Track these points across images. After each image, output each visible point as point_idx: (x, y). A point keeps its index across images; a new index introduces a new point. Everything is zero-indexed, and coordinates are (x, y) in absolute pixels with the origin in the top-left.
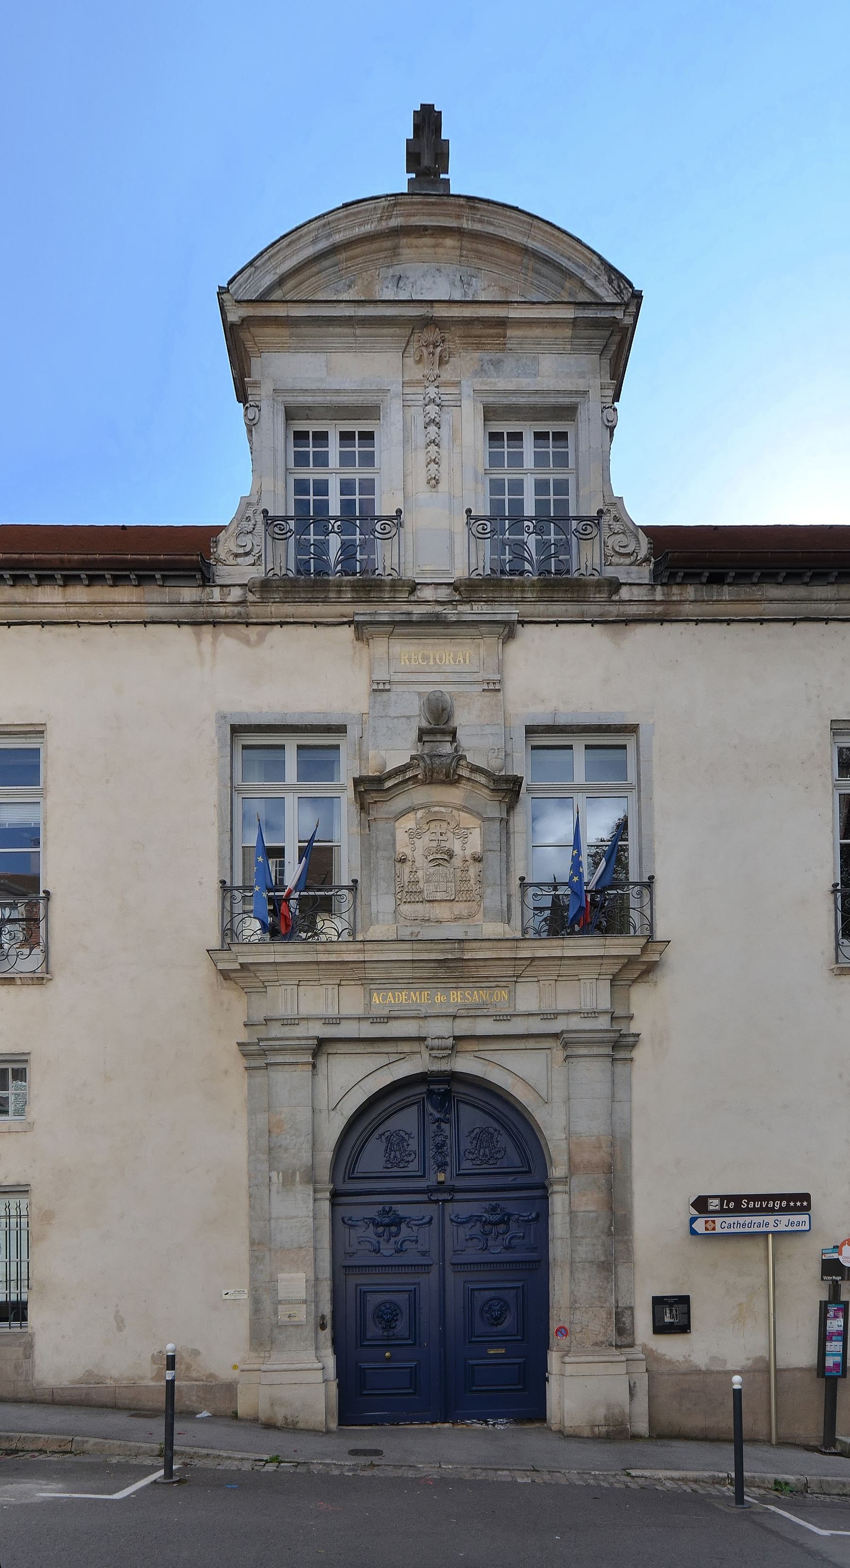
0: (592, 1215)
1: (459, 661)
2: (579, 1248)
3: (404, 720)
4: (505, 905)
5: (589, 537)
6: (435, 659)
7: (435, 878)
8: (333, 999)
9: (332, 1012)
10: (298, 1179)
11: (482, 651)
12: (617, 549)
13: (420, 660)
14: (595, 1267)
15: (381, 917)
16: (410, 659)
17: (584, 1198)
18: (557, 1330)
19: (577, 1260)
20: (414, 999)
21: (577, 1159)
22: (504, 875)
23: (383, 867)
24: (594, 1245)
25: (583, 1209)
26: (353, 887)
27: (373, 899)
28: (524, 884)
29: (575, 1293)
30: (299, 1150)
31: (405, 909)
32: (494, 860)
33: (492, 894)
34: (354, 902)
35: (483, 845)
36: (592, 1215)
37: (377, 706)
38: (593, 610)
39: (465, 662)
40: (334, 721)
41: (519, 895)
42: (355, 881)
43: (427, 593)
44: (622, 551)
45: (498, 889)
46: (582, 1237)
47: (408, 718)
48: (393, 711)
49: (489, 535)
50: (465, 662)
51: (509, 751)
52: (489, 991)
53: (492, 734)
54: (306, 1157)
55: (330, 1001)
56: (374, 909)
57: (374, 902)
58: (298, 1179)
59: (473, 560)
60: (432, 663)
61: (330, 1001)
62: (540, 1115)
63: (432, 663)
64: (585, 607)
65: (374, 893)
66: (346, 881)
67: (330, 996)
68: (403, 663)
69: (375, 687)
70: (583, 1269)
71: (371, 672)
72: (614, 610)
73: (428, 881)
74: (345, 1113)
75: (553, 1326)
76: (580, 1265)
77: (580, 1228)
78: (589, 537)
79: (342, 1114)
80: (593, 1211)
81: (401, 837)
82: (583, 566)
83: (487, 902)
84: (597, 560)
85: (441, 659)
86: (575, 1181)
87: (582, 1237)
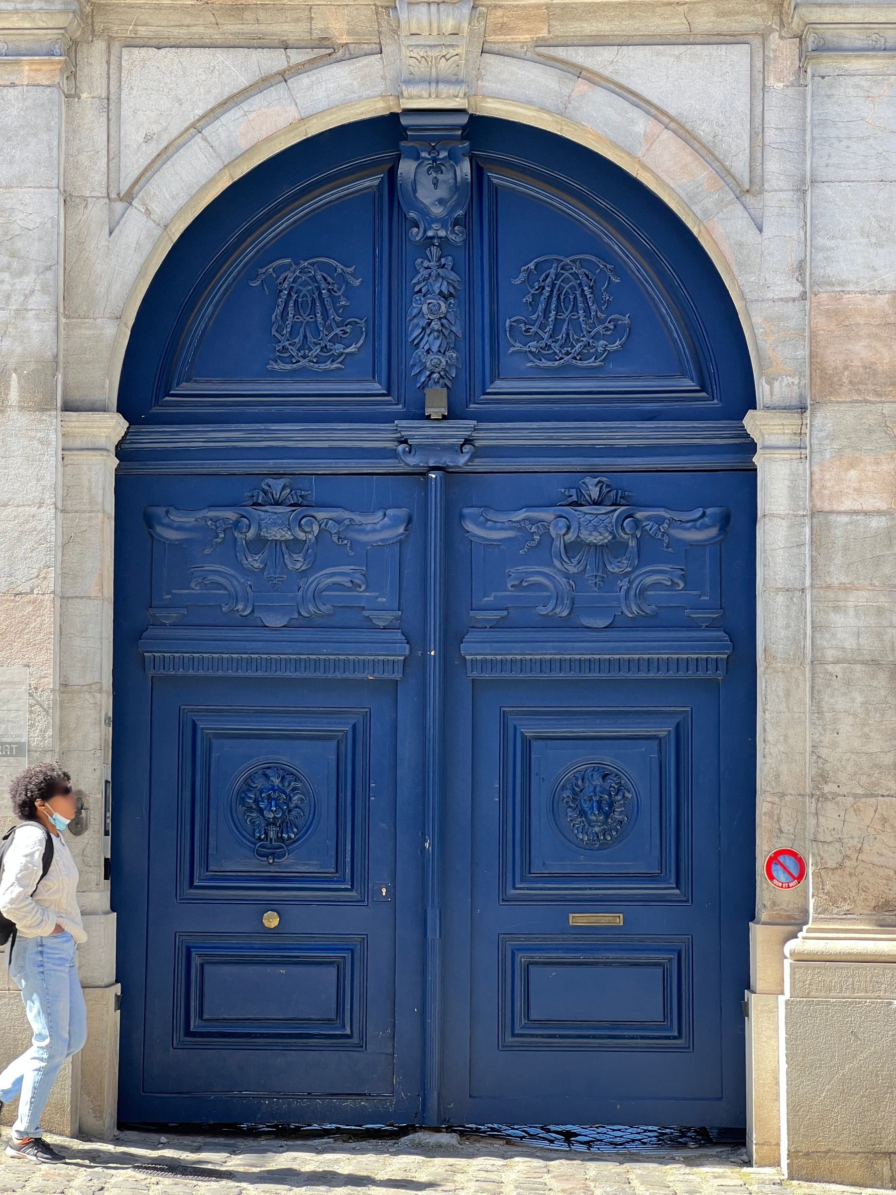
0: (875, 523)
2: (837, 619)
10: (14, 395)
14: (882, 678)
17: (853, 474)
18: (773, 860)
19: (830, 654)
21: (833, 358)
24: (880, 611)
25: (847, 504)
29: (824, 752)
30: (20, 313)
36: (875, 523)
46: (845, 588)
54: (37, 332)
58: (14, 395)
62: (721, 233)
70: (848, 683)
74: (157, 209)
75: (764, 849)
76: (837, 669)
77: (838, 559)
79: (148, 212)
80: (879, 513)
86: (825, 420)
87: (845, 588)
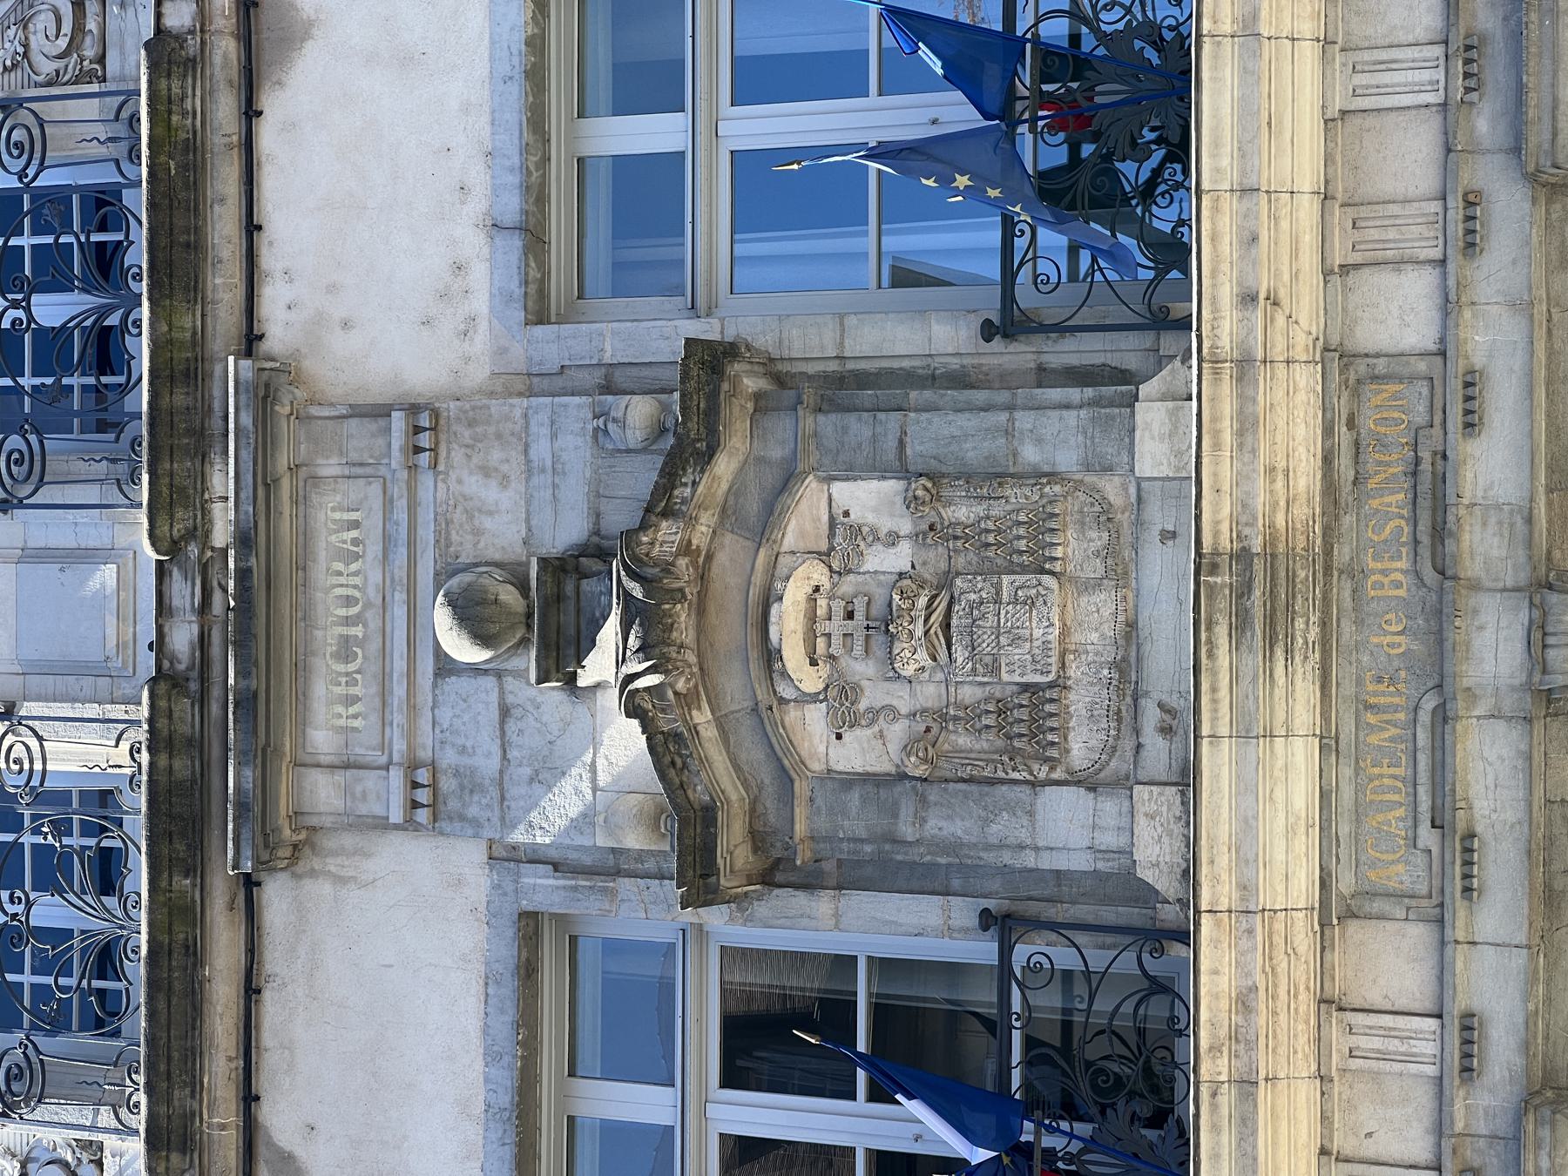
1: (356, 542)
3: (511, 726)
4: (1075, 394)
5: (36, 132)
6: (347, 621)
7: (986, 644)
8: (1388, 1033)
9: (1424, 1040)
11: (329, 467)
12: (63, 43)
13: (352, 667)
15: (1109, 840)
16: (350, 700)
20: (1393, 731)
22: (980, 396)
23: (950, 823)
26: (1003, 925)
27: (1047, 862)
28: (1008, 324)
31: (1081, 746)
32: (937, 431)
33: (1039, 441)
34: (1054, 926)
35: (883, 473)
37: (473, 811)
38: (225, 110)
39: (355, 525)
40: (508, 952)
41: (1038, 339)
42: (987, 919)
43: (182, 637)
44: (67, 28)
45: (1024, 420)
47: (505, 712)
48: (489, 764)
49: (33, 438)
50: (355, 525)
51: (597, 377)
52: (1371, 458)
53: (554, 436)
55: (1393, 1045)
56: (1080, 862)
57: (1062, 862)
59: (90, 494)
60: (358, 631)
61: (1393, 1045)
63: (358, 631)
64: (217, 141)
65: (1029, 860)
66: (985, 950)
67: (1376, 1043)
68: (357, 723)
69: (422, 815)
71: (382, 825)
72: (225, 49)
73: (994, 669)
78: (36, 132)
81: (857, 753)
82: (103, 151)
83: (1067, 459)
84: (91, 108)
85: (349, 601)
